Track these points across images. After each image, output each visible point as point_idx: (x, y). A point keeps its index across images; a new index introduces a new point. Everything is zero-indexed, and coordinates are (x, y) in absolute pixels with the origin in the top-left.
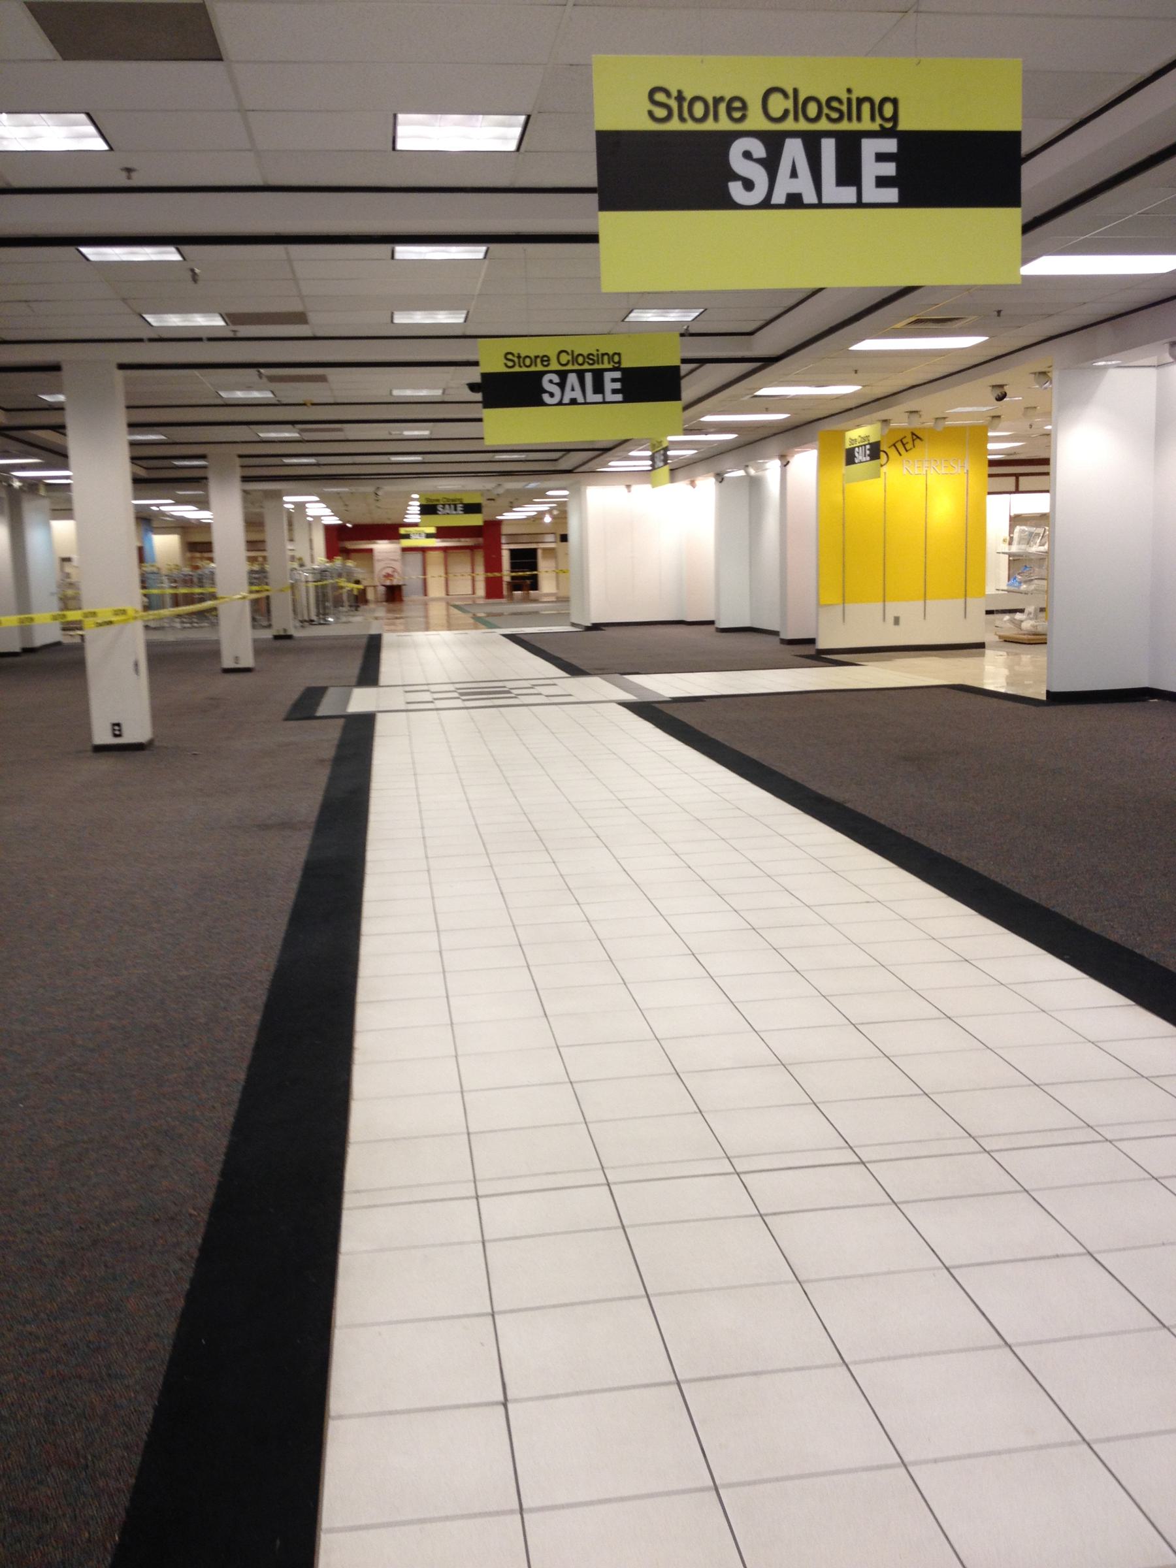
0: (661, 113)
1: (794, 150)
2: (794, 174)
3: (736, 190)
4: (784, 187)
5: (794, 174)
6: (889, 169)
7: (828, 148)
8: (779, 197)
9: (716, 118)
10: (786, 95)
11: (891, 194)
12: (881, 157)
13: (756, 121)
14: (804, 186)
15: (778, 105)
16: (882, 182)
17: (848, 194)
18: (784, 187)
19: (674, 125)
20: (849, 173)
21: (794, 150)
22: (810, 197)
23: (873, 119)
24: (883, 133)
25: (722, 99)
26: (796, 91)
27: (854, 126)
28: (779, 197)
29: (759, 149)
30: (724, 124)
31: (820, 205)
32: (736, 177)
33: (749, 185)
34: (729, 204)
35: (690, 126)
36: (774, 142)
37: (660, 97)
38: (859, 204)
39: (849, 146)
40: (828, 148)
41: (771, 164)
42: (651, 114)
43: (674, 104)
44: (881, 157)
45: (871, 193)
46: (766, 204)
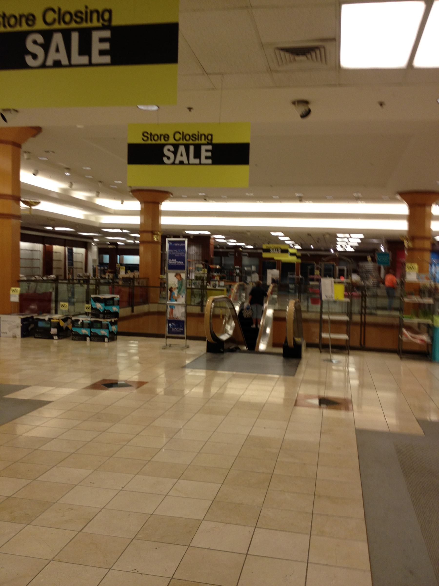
0: (145, 138)
1: (182, 149)
2: (182, 155)
3: (165, 160)
5: (182, 155)
6: (209, 154)
7: (192, 148)
8: (177, 162)
9: (160, 140)
10: (180, 133)
16: (207, 158)
17: (197, 161)
18: (179, 158)
19: (149, 142)
20: (197, 155)
21: (182, 149)
23: (205, 140)
24: (208, 144)
25: (162, 135)
26: (183, 133)
27: (200, 142)
28: (177, 162)
29: (172, 148)
30: (163, 142)
31: (189, 164)
32: (165, 156)
34: (163, 163)
35: (153, 142)
37: (146, 134)
38: (200, 164)
40: (192, 148)
41: (175, 153)
42: (143, 139)
43: (149, 136)
44: (207, 151)
45: (204, 161)
46: (174, 163)
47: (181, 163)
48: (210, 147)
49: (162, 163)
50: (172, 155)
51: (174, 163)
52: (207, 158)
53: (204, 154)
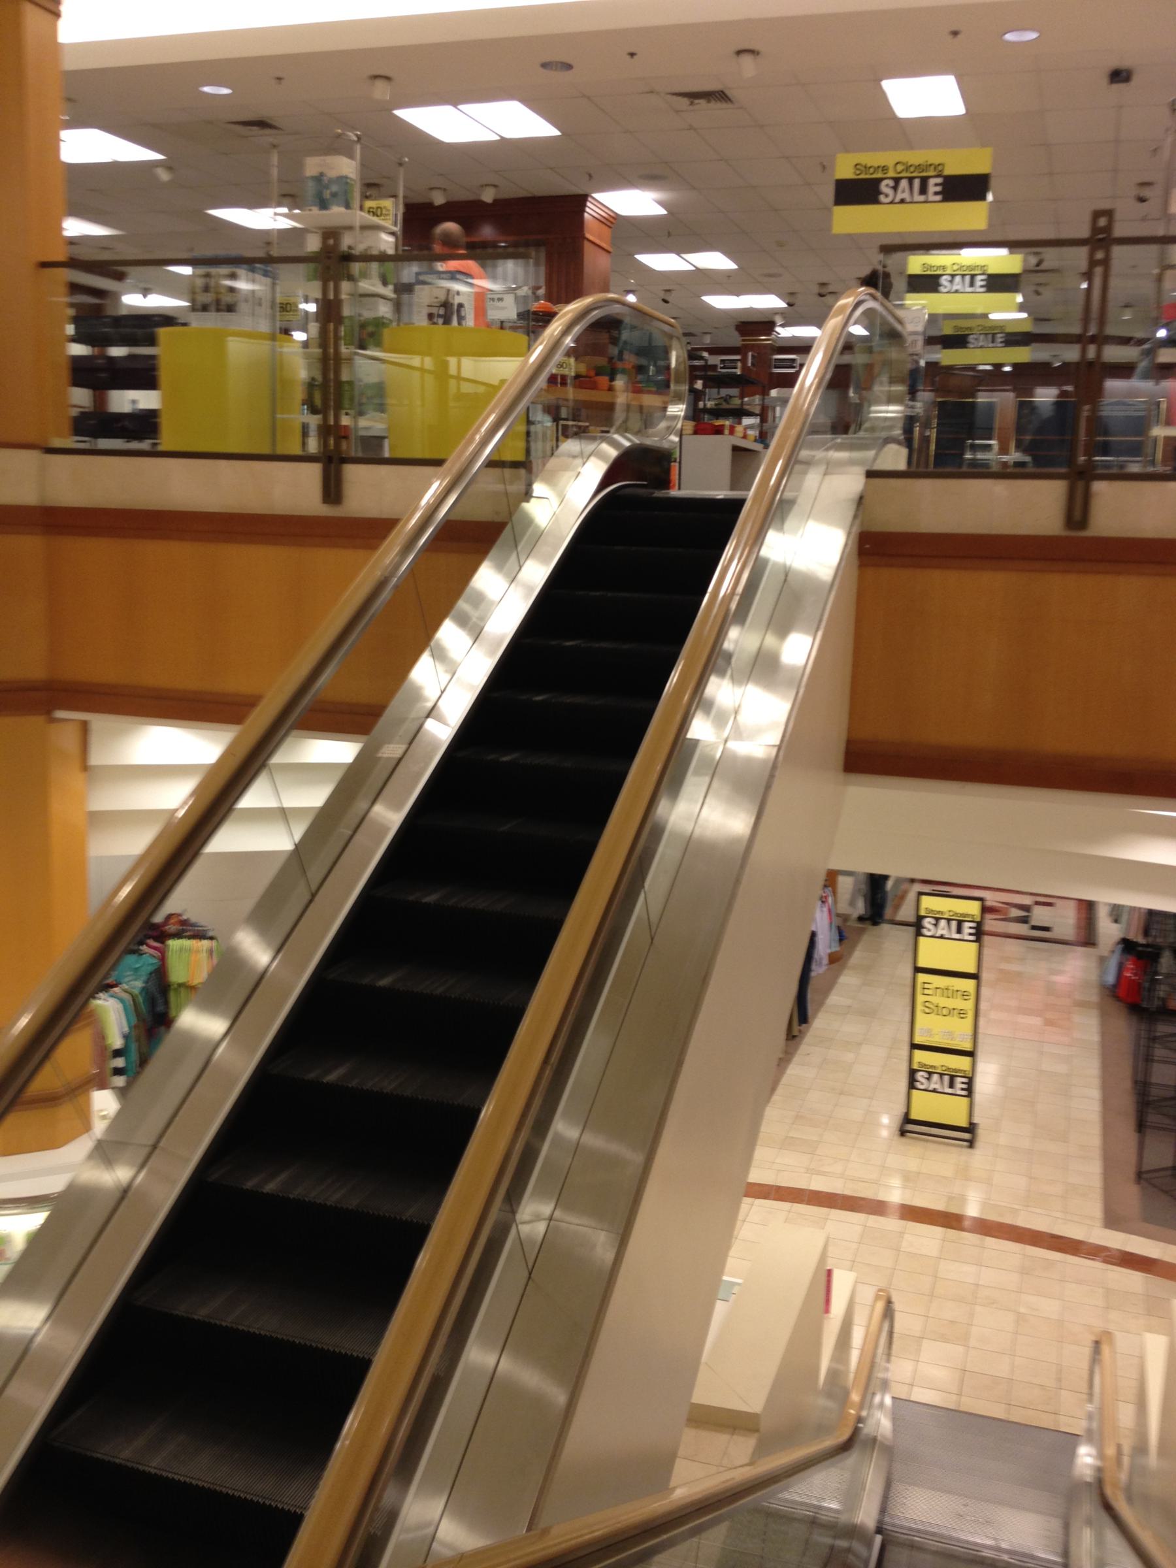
1: (904, 184)
4: (899, 197)
6: (939, 189)
8: (897, 200)
11: (939, 198)
12: (936, 185)
13: (891, 174)
14: (906, 196)
15: (900, 168)
16: (936, 193)
17: (922, 198)
19: (863, 176)
20: (923, 190)
21: (904, 184)
22: (908, 200)
29: (891, 183)
30: (879, 175)
33: (887, 196)
35: (868, 176)
36: (897, 181)
38: (926, 202)
39: (924, 181)
40: (917, 183)
41: (895, 188)
44: (936, 185)
47: (902, 201)
48: (939, 180)
49: (876, 201)
50: (890, 192)
51: (892, 203)
52: (936, 193)
53: (932, 189)
